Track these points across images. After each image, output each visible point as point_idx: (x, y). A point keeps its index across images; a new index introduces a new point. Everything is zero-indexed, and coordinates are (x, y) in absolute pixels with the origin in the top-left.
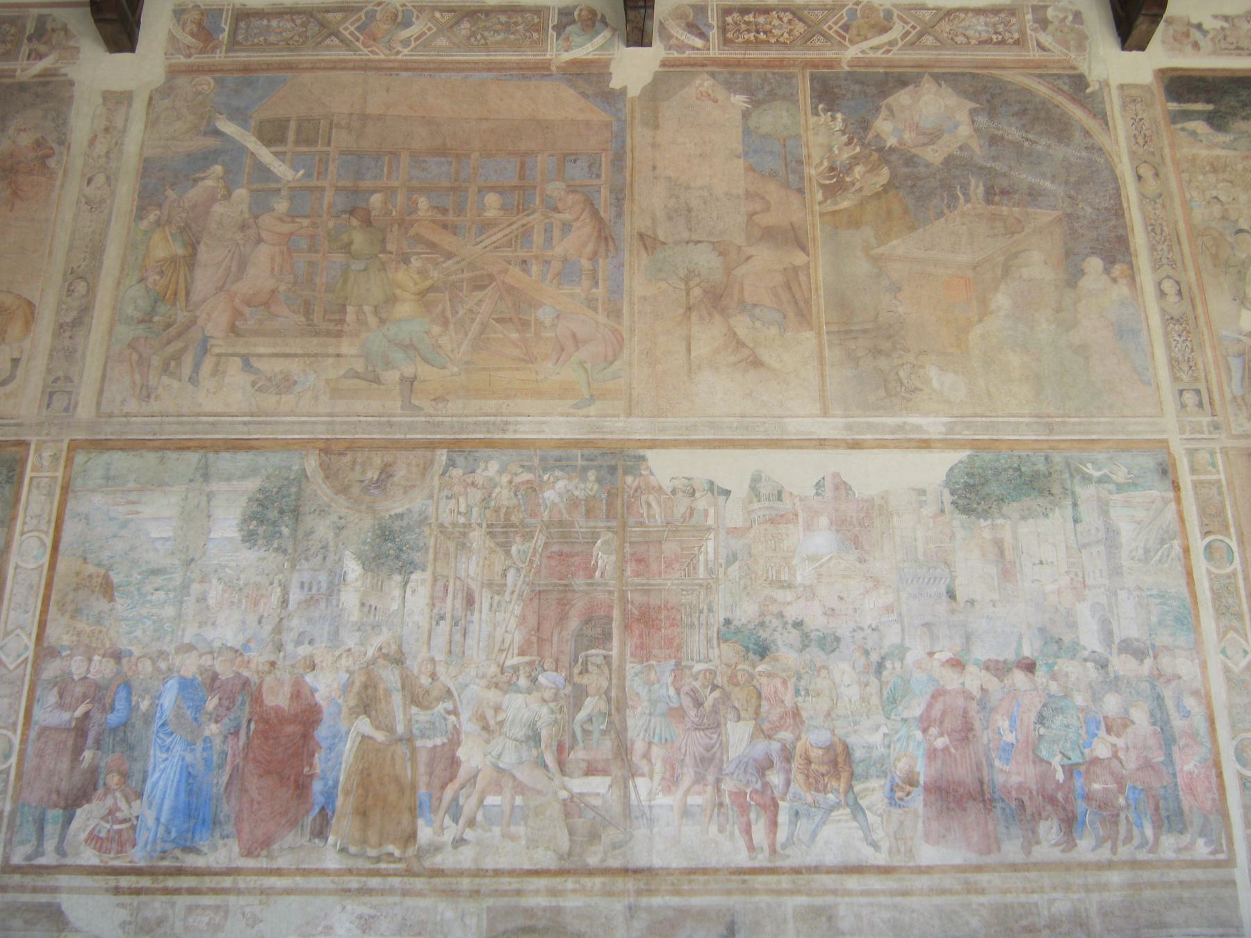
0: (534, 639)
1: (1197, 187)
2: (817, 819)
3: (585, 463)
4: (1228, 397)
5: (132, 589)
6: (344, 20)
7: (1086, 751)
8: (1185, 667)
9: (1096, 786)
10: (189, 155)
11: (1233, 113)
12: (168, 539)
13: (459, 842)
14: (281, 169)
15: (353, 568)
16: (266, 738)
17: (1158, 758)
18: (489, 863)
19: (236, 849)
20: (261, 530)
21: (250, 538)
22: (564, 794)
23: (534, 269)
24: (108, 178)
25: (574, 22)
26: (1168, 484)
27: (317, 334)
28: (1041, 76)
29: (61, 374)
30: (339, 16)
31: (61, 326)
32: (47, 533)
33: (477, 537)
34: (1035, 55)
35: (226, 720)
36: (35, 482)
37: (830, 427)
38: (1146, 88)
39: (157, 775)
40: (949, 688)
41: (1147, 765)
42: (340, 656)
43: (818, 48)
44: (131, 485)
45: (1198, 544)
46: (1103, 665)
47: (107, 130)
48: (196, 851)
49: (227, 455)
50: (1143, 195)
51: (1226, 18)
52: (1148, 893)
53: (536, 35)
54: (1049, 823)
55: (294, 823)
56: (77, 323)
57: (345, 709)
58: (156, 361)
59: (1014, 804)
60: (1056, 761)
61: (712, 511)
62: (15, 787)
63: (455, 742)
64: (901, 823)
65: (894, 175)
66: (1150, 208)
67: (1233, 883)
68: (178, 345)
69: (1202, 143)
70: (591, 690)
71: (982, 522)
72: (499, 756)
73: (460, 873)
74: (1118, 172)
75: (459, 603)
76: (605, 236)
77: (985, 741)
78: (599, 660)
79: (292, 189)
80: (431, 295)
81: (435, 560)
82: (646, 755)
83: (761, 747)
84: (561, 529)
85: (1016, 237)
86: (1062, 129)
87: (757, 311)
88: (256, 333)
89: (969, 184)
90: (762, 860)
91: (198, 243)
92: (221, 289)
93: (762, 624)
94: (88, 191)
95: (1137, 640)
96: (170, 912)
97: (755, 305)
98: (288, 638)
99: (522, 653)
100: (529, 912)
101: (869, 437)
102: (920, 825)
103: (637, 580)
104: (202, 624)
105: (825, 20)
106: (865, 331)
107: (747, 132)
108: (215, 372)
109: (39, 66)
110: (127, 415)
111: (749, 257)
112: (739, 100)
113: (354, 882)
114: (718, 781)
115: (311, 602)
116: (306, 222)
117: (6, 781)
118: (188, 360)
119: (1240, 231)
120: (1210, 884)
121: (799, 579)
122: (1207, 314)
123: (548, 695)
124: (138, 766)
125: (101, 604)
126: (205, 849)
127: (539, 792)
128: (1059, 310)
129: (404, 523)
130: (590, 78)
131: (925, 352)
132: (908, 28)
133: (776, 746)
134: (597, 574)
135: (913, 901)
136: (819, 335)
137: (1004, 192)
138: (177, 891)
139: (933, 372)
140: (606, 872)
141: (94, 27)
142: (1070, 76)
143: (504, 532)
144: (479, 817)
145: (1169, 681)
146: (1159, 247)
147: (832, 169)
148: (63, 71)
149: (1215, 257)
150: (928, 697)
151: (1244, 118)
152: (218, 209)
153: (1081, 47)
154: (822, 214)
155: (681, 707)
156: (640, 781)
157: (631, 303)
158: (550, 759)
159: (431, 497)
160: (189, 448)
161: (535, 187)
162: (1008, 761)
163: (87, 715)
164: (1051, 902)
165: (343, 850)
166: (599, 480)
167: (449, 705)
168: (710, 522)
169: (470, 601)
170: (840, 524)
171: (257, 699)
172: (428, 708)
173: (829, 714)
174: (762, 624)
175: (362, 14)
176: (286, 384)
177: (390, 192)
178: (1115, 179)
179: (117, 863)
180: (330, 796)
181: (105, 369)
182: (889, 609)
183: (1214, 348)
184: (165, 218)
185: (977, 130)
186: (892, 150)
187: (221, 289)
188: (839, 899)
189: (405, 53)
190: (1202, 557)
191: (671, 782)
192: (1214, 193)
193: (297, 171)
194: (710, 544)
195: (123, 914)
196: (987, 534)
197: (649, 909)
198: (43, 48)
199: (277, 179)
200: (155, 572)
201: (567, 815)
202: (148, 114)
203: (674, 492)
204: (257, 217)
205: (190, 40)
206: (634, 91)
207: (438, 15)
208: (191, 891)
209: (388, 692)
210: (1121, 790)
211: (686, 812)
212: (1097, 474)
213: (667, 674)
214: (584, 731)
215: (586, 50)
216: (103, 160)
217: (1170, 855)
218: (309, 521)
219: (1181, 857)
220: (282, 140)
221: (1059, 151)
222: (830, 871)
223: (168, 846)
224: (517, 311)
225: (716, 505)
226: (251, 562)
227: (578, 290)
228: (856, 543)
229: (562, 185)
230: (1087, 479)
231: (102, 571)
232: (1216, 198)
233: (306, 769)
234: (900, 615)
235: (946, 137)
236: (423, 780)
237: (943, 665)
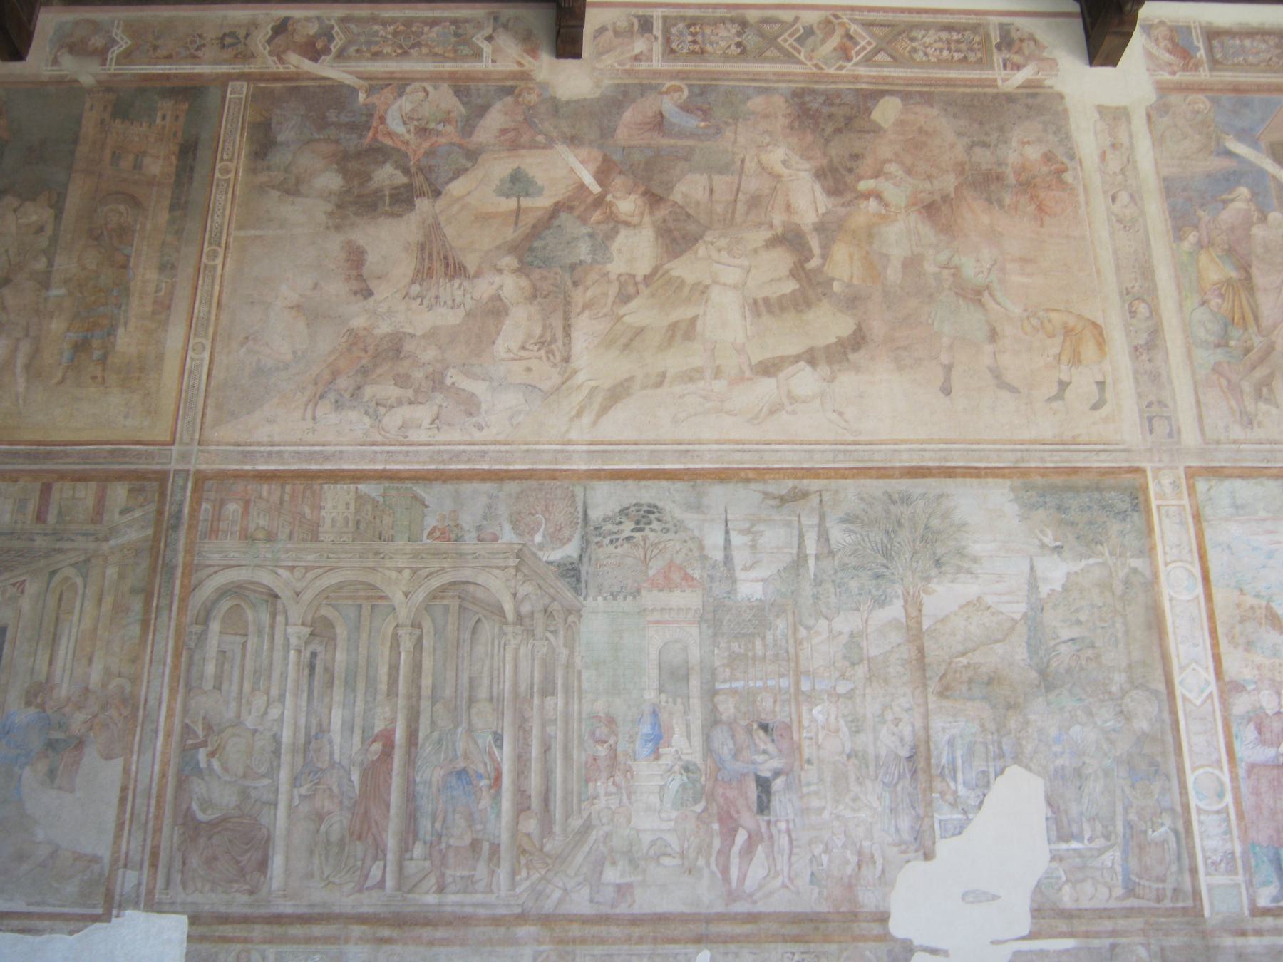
10: (1209, 176)
24: (1132, 196)
31: (1136, 348)
32: (1192, 563)
36: (1163, 510)
44: (1262, 514)
47: (1113, 146)
58: (1247, 387)
62: (1239, 826)
91: (1250, 266)
109: (1020, 77)
110: (1235, 442)
117: (1228, 819)
148: (1047, 83)
152: (1258, 231)
181: (1196, 393)
184: (1206, 240)
198: (1017, 58)
202: (1151, 132)
205: (1167, 57)
216: (1120, 177)
231: (1264, 603)
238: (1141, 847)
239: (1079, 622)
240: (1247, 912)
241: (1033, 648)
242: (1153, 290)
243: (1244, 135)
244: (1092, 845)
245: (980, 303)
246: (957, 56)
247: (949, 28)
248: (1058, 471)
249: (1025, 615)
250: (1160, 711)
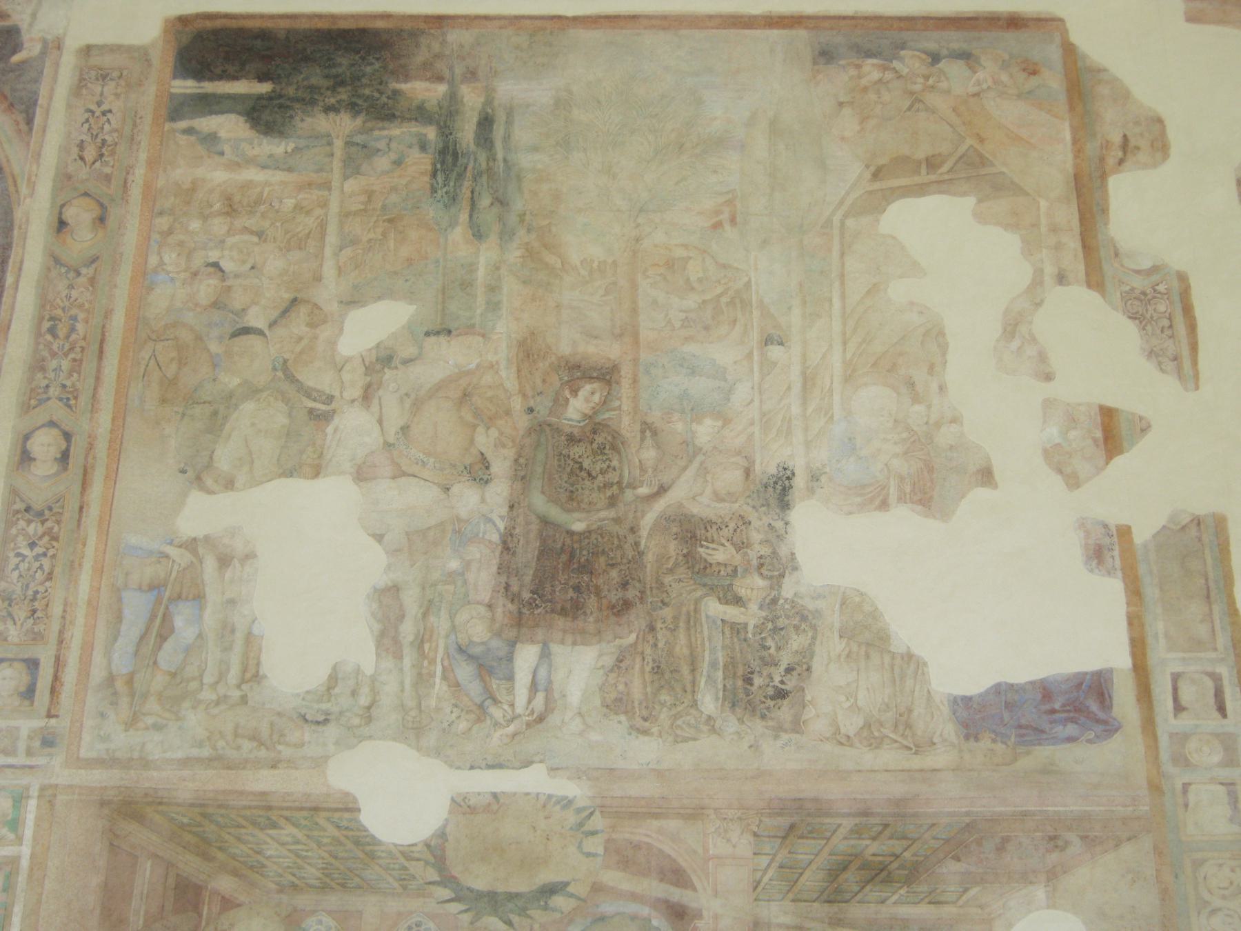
1: (181, 244)
4: (98, 674)
11: (309, 100)
38: (141, 54)
50: (57, 261)
66: (61, 286)
74: (18, 214)
119: (246, 331)
122: (109, 503)
146: (53, 364)
149: (170, 384)
151: (328, 109)
183: (99, 570)
192: (214, 256)
232: (216, 265)
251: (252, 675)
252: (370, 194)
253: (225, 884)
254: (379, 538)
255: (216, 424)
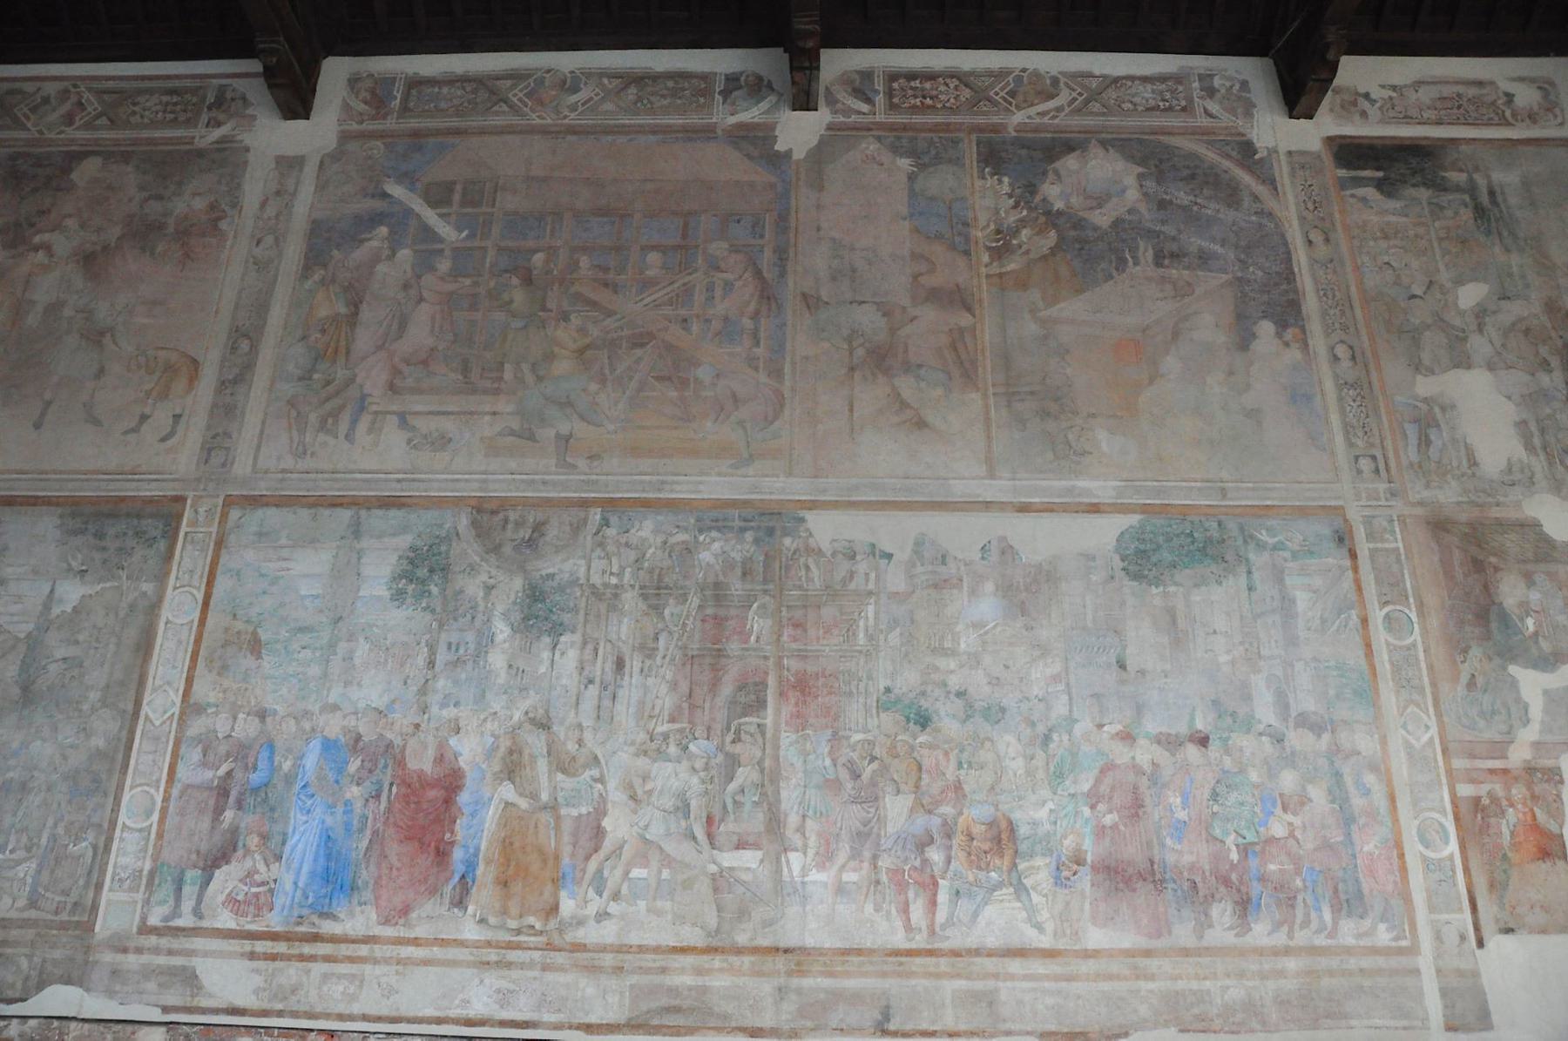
0: (685, 705)
2: (979, 899)
3: (742, 524)
4: (1405, 462)
5: (278, 646)
6: (513, 87)
7: (1262, 829)
8: (1365, 743)
9: (1272, 867)
12: (317, 597)
13: (602, 916)
14: (445, 230)
15: (502, 630)
16: (408, 803)
17: (1337, 837)
18: (634, 939)
19: (374, 916)
20: (411, 588)
21: (399, 596)
22: (713, 868)
23: (695, 328)
24: (277, 239)
25: (741, 87)
26: (1345, 551)
27: (474, 391)
28: (1209, 143)
29: (220, 430)
30: (509, 83)
32: (198, 589)
33: (630, 599)
34: (1204, 122)
35: (367, 783)
37: (998, 489)
39: (297, 837)
40: (1118, 762)
41: (1326, 846)
42: (485, 720)
43: (985, 114)
44: (284, 541)
45: (1378, 615)
46: (1279, 740)
47: (278, 193)
48: (334, 918)
49: (380, 512)
51: (1394, 88)
52: (1326, 982)
53: (702, 100)
54: (1222, 905)
55: (433, 891)
56: (236, 381)
57: (489, 775)
59: (1186, 885)
60: (1230, 840)
61: (873, 575)
63: (600, 812)
64: (1068, 903)
65: (1062, 238)
67: (1416, 972)
68: (337, 401)
69: (1370, 208)
70: (743, 759)
71: (1154, 590)
72: (647, 826)
73: (603, 949)
75: (609, 666)
76: (768, 296)
77: (1157, 817)
78: (753, 729)
79: (455, 250)
80: (589, 353)
81: (586, 621)
82: (801, 830)
83: (921, 821)
84: (717, 592)
85: (1186, 300)
86: (1232, 194)
87: (922, 372)
88: (418, 391)
89: (1137, 248)
90: (920, 941)
92: (380, 348)
93: (923, 694)
94: (257, 251)
95: (1315, 713)
96: (304, 979)
97: (920, 366)
98: (434, 700)
99: (672, 720)
100: (673, 991)
101: (1037, 500)
102: (1087, 906)
103: (794, 646)
104: (347, 684)
105: (992, 86)
106: (1032, 393)
107: (912, 194)
108: (370, 431)
110: (283, 471)
111: (915, 318)
112: (905, 163)
113: (492, 955)
114: (875, 857)
115: (457, 663)
116: (468, 282)
118: (345, 418)
119: (1414, 296)
120: (1393, 972)
121: (963, 646)
123: (699, 764)
124: (278, 828)
125: (248, 662)
126: (342, 916)
127: (688, 866)
128: (1231, 373)
129: (555, 584)
130: (756, 141)
131: (1093, 416)
132: (1074, 95)
133: (937, 821)
134: (753, 638)
135: (1077, 987)
136: (985, 396)
137: (1173, 256)
138: (312, 958)
139: (1102, 435)
140: (755, 950)
141: (267, 92)
142: (1241, 144)
143: (656, 592)
144: (624, 890)
145: (1347, 757)
146: (1332, 312)
147: (998, 232)
150: (1096, 771)
151: (1414, 186)
152: (381, 268)
153: (1248, 114)
154: (988, 276)
155: (837, 779)
156: (792, 856)
157: (794, 364)
158: (700, 833)
159: (584, 557)
160: (341, 505)
161: (697, 247)
162: (1180, 840)
163: (229, 774)
164: (1225, 989)
165: (482, 921)
166: (757, 541)
167: (595, 773)
168: (871, 586)
169: (620, 664)
170: (1006, 589)
171: (401, 763)
172: (574, 775)
173: (993, 788)
174: (923, 694)
175: (531, 80)
176: (442, 442)
177: (552, 251)
178: (1286, 244)
179: (253, 927)
180: (471, 865)
182: (1056, 678)
185: (1145, 194)
186: (1060, 213)
187: (380, 348)
188: (1001, 984)
189: (572, 119)
190: (1381, 627)
191: (825, 857)
192: (1386, 259)
193: (461, 232)
194: (871, 609)
195: (258, 980)
196: (1157, 601)
197: (799, 991)
198: (221, 117)
199: (442, 241)
200: (301, 630)
201: (716, 890)
203: (834, 554)
204: (419, 277)
205: (362, 107)
206: (798, 155)
207: (606, 81)
208: (328, 959)
209: (533, 758)
210: (1298, 872)
211: (841, 889)
212: (1271, 541)
213: (824, 743)
214: (735, 802)
215: (751, 114)
217: (1350, 941)
218: (460, 581)
219: (1362, 943)
220: (449, 203)
221: (1227, 215)
222: (991, 954)
223: (305, 912)
224: (676, 370)
225: (877, 569)
226: (402, 621)
227: (739, 349)
228: (1024, 610)
229: (725, 245)
230: (1261, 546)
231: (251, 629)
233: (448, 835)
234: (1068, 685)
235: (1115, 200)
236: (567, 850)
237: (1112, 738)
238: (57, 861)
239: (77, 642)
240: (135, 930)
241: (25, 666)
242: (260, 329)
243: (408, 179)
244: (13, 856)
245: (99, 344)
246: (170, 116)
247: (172, 92)
248: (108, 500)
249: (29, 635)
250: (121, 728)
251: (1473, 463)
252: (1448, 229)
253: (1493, 560)
254: (1509, 398)
255: (1416, 343)
